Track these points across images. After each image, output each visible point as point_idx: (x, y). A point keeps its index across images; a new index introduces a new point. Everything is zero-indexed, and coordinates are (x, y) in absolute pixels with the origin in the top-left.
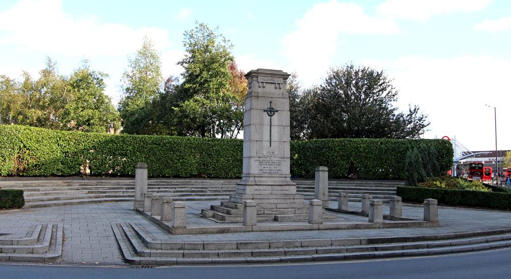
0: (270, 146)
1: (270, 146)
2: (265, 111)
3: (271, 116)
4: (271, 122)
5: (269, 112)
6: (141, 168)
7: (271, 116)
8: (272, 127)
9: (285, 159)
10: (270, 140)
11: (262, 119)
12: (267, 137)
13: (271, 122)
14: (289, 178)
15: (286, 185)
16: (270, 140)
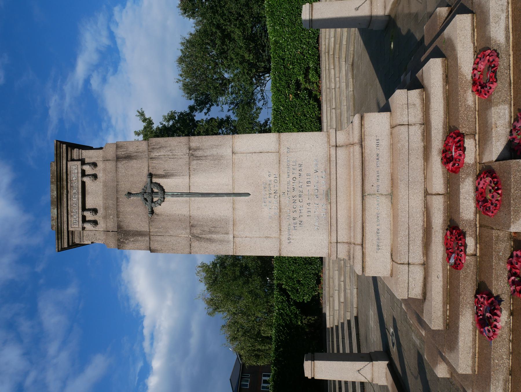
0: (248, 194)
1: (248, 194)
2: (152, 212)
4: (182, 195)
6: (313, 370)
8: (193, 190)
9: (284, 150)
13: (182, 195)
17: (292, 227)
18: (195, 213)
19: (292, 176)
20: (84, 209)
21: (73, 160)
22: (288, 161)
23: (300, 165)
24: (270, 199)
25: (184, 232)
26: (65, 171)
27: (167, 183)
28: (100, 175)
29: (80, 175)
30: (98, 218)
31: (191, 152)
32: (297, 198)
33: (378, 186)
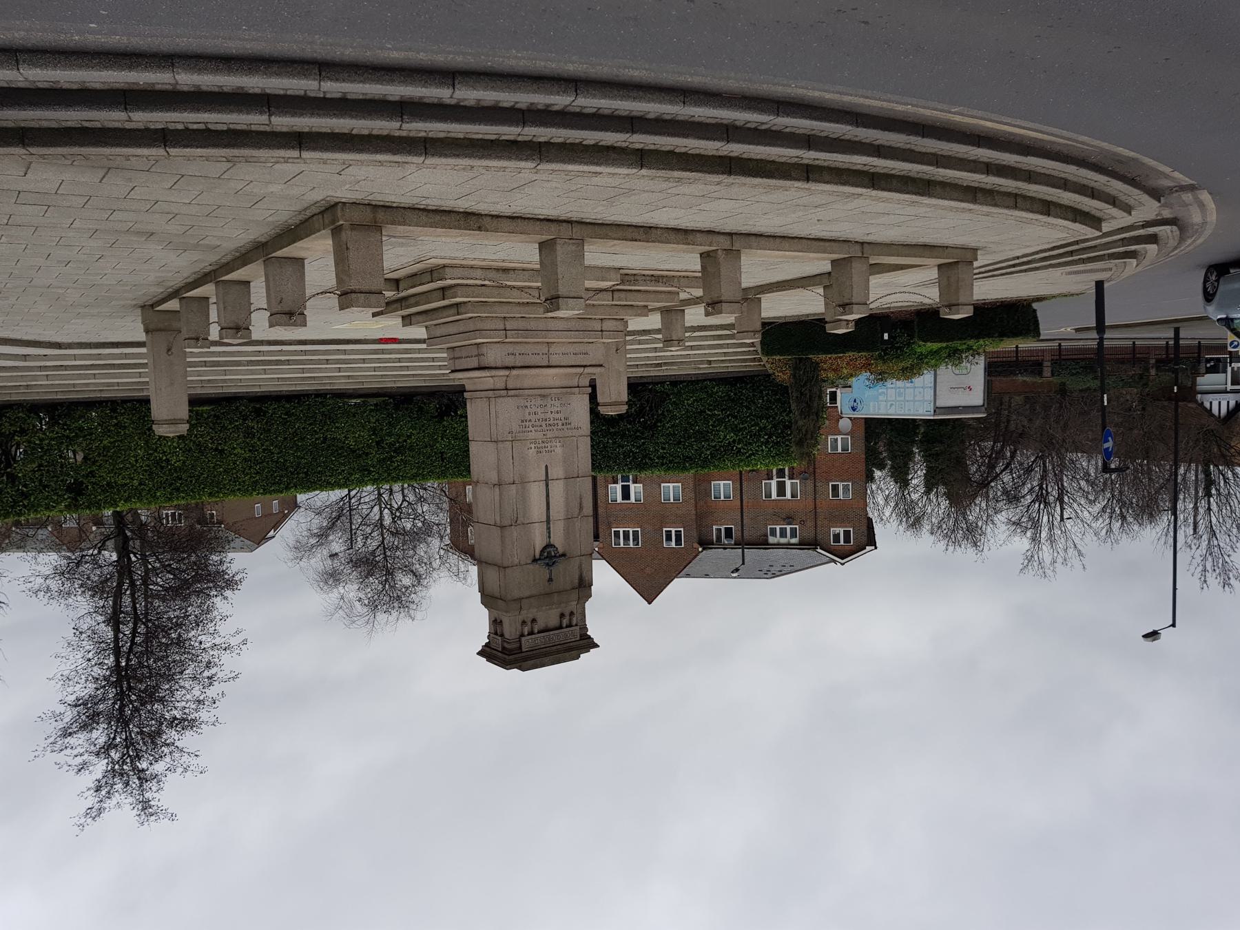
2: (564, 555)
3: (549, 545)
4: (549, 528)
5: (553, 554)
7: (549, 545)
8: (544, 518)
10: (547, 485)
11: (568, 532)
12: (557, 489)
13: (549, 528)
14: (467, 388)
15: (514, 368)
16: (547, 485)
17: (569, 426)
18: (562, 516)
20: (561, 627)
21: (520, 647)
22: (519, 432)
23: (522, 421)
24: (549, 447)
25: (577, 524)
26: (531, 653)
27: (539, 543)
28: (531, 616)
29: (533, 636)
30: (567, 614)
31: (513, 524)
33: (543, 354)
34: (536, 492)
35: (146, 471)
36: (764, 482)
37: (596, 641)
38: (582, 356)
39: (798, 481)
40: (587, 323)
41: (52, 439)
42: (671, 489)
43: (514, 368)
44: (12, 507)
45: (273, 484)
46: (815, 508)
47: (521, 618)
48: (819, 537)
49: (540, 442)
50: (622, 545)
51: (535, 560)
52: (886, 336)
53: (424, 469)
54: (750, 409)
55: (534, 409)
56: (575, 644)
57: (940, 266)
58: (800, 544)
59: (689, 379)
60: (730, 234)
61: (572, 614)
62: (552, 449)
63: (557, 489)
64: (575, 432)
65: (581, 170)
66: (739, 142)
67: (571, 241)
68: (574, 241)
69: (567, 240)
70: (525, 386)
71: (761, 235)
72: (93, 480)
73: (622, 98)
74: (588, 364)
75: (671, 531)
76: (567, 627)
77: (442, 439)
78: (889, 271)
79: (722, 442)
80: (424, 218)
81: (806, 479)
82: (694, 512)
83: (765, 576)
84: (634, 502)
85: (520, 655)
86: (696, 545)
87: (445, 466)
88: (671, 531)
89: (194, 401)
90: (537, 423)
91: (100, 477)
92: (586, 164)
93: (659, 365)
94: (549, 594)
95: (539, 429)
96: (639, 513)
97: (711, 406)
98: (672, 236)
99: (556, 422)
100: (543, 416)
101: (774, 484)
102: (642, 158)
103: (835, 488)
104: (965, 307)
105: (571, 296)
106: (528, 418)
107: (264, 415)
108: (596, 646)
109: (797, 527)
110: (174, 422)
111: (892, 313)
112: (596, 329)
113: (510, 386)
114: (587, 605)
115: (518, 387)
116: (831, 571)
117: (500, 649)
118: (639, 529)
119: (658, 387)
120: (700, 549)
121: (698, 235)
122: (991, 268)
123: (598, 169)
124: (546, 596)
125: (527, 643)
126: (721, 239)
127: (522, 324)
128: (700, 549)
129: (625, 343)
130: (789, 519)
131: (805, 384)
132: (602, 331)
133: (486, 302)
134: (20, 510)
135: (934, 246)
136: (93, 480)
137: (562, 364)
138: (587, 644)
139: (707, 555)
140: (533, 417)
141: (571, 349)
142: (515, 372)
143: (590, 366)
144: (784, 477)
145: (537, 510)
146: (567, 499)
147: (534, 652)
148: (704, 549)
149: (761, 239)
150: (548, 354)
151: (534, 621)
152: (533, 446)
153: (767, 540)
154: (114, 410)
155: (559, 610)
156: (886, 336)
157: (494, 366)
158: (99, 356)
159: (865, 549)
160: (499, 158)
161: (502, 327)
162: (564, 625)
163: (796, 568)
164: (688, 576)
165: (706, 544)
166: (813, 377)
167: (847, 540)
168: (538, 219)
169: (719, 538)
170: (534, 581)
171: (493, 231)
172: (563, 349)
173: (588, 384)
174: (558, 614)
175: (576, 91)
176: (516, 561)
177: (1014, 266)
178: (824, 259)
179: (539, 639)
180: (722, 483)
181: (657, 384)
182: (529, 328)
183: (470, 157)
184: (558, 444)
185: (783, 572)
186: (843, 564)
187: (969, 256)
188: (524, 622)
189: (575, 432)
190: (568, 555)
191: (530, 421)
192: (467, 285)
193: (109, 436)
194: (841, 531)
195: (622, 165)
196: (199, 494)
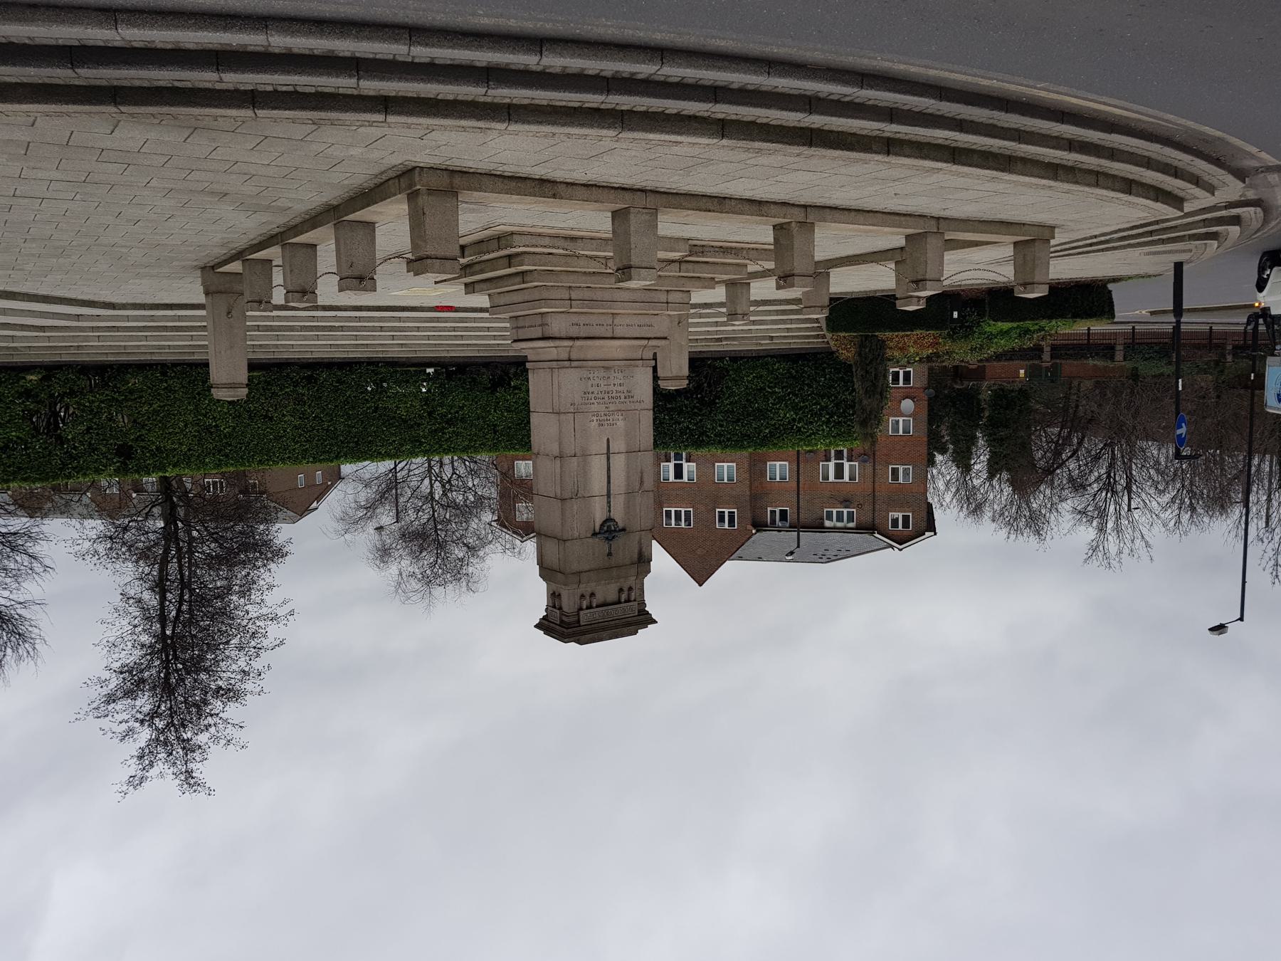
0: (608, 439)
1: (608, 439)
2: (623, 530)
3: (609, 520)
4: (609, 502)
5: (613, 528)
7: (609, 520)
10: (608, 459)
11: (628, 507)
12: (619, 462)
13: (609, 502)
16: (608, 459)
17: (631, 400)
18: (623, 490)
19: (593, 401)
20: (619, 602)
21: (579, 621)
23: (585, 393)
26: (589, 627)
27: (599, 517)
28: (590, 590)
29: (592, 610)
31: (574, 497)
32: (610, 395)
34: (598, 465)
35: (195, 436)
36: (821, 463)
37: (654, 617)
38: (647, 328)
39: (857, 464)
40: (653, 294)
41: (102, 402)
42: (726, 469)
43: (578, 338)
44: (61, 469)
45: (324, 452)
46: (874, 491)
47: (579, 592)
48: (877, 521)
49: (602, 415)
50: (673, 525)
51: (595, 534)
52: (955, 315)
53: (475, 441)
54: (812, 387)
55: (597, 381)
56: (635, 618)
57: (1015, 244)
58: (857, 528)
59: (750, 355)
60: (805, 207)
61: (630, 589)
62: (615, 422)
63: (619, 462)
64: (637, 406)
65: (662, 139)
66: (822, 114)
67: (644, 211)
68: (646, 211)
69: (640, 210)
70: (589, 357)
71: (836, 208)
72: (142, 444)
73: (708, 68)
74: (653, 336)
75: (724, 512)
76: (626, 602)
77: (495, 411)
78: (964, 248)
79: (781, 420)
80: (499, 183)
81: (866, 462)
82: (748, 493)
83: (820, 560)
84: (687, 481)
85: (578, 629)
86: (749, 527)
87: (497, 439)
88: (724, 512)
89: (253, 366)
90: (600, 395)
91: (149, 441)
92: (668, 133)
93: (720, 340)
94: (609, 568)
95: (601, 401)
96: (692, 493)
97: (771, 383)
98: (747, 207)
99: (618, 395)
100: (605, 388)
101: (832, 465)
102: (723, 128)
103: (895, 472)
104: (1040, 286)
105: (643, 266)
106: (591, 390)
107: (315, 382)
108: (655, 622)
109: (855, 510)
110: (232, 386)
111: (963, 290)
112: (662, 301)
113: (574, 356)
114: (646, 580)
115: (582, 358)
116: (888, 558)
117: (558, 623)
118: (691, 509)
119: (718, 364)
120: (754, 531)
121: (772, 206)
122: (1067, 246)
123: (679, 138)
124: (607, 569)
125: (585, 616)
126: (796, 211)
127: (588, 294)
128: (754, 531)
129: (688, 316)
130: (846, 502)
131: (871, 362)
132: (667, 303)
133: (552, 271)
134: (70, 473)
135: (1012, 223)
136: (142, 444)
137: (626, 336)
138: (644, 619)
139: (760, 537)
140: (595, 389)
141: (636, 320)
142: (578, 343)
143: (655, 338)
144: (843, 460)
145: (597, 484)
146: (628, 473)
147: (593, 626)
148: (758, 531)
149: (834, 212)
150: (613, 325)
151: (592, 595)
152: (595, 418)
153: (823, 523)
154: (164, 374)
155: (618, 584)
156: (955, 315)
157: (558, 336)
158: (152, 318)
159: (924, 534)
160: (582, 125)
161: (567, 296)
162: (623, 600)
163: (851, 553)
164: (740, 558)
165: (760, 526)
166: (879, 355)
167: (906, 524)
168: (612, 188)
169: (773, 521)
170: (594, 554)
171: (566, 199)
172: (628, 321)
173: (652, 357)
174: (617, 589)
175: (662, 60)
176: (576, 534)
177: (1091, 245)
178: (898, 234)
179: (597, 614)
180: (778, 463)
181: (715, 359)
182: (595, 298)
183: (553, 124)
184: (621, 417)
185: (838, 557)
186: (901, 550)
187: (1047, 234)
188: (582, 596)
189: (637, 406)
190: (628, 529)
191: (592, 393)
192: (534, 253)
193: (159, 400)
194: (900, 515)
195: (703, 135)
196: (248, 462)
